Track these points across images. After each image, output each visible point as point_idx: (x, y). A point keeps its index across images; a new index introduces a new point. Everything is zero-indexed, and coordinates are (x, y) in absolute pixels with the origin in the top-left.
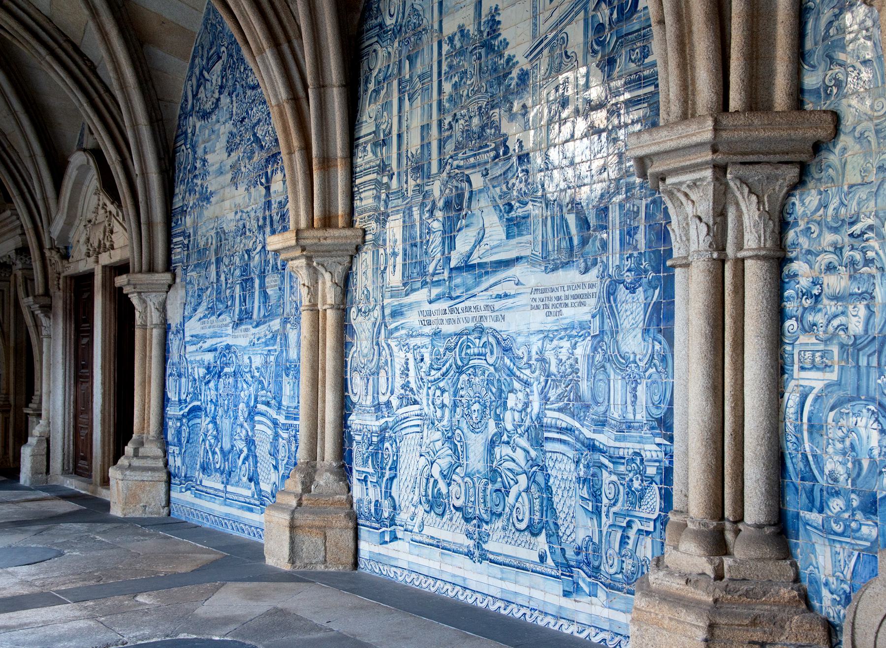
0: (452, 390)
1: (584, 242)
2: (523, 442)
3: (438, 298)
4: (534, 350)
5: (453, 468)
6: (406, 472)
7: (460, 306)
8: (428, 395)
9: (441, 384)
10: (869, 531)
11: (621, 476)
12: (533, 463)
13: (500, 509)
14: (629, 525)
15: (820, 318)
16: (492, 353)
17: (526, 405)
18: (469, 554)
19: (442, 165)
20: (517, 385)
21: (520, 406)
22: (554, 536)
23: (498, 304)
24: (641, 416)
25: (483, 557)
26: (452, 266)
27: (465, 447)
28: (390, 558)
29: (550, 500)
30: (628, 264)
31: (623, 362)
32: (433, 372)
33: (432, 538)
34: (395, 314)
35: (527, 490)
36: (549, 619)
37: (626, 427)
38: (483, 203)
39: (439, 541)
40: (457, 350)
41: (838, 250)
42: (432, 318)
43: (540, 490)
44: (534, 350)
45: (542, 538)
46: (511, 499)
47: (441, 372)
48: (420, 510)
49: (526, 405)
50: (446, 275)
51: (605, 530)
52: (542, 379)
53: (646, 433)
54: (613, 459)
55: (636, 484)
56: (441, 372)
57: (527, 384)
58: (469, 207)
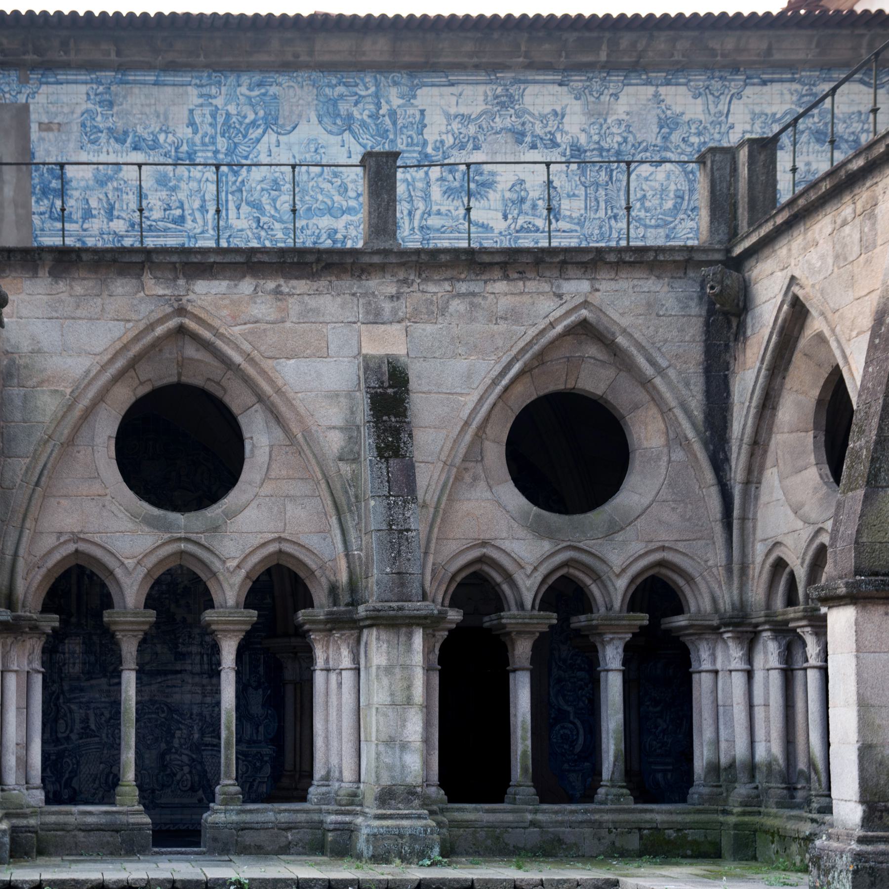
4: (195, 712)
35: (190, 772)
46: (178, 777)
55: (258, 764)
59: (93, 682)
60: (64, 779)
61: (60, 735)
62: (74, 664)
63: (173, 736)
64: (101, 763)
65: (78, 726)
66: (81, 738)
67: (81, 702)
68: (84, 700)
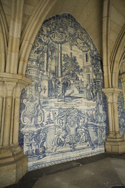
0: (65, 120)
1: (94, 97)
2: (84, 127)
3: (61, 101)
4: (85, 112)
5: (66, 135)
6: (50, 139)
7: (67, 103)
8: (58, 121)
9: (62, 119)
10: (124, 129)
11: (100, 129)
12: (86, 130)
13: (79, 140)
14: (102, 136)
15: (119, 110)
16: (76, 112)
17: (84, 121)
18: (71, 151)
19: (62, 76)
20: (82, 118)
21: (83, 121)
22: (90, 141)
23: (77, 104)
24: (103, 121)
25: (75, 150)
26: (65, 95)
27: (69, 130)
28: (42, 162)
29: (89, 136)
30: (100, 101)
31: (100, 114)
32: (59, 116)
33: (59, 151)
34: (44, 103)
36: (90, 155)
37: (101, 122)
38: (73, 86)
39: (62, 151)
40: (67, 112)
41: (120, 104)
42: (59, 105)
43: (87, 134)
44: (85, 112)
45: (88, 142)
46: (81, 138)
47: (62, 116)
48: (55, 147)
49: (84, 121)
50: (63, 97)
51: (98, 137)
52: (87, 117)
53: (103, 123)
54: (99, 127)
55: (102, 130)
56: (62, 116)
57: (84, 118)
58: (70, 86)
59: (52, 100)
60: (40, 143)
61: (39, 123)
62: (45, 92)
63: (79, 122)
64: (55, 134)
65: (46, 119)
66: (47, 124)
67: (48, 108)
68: (48, 107)
